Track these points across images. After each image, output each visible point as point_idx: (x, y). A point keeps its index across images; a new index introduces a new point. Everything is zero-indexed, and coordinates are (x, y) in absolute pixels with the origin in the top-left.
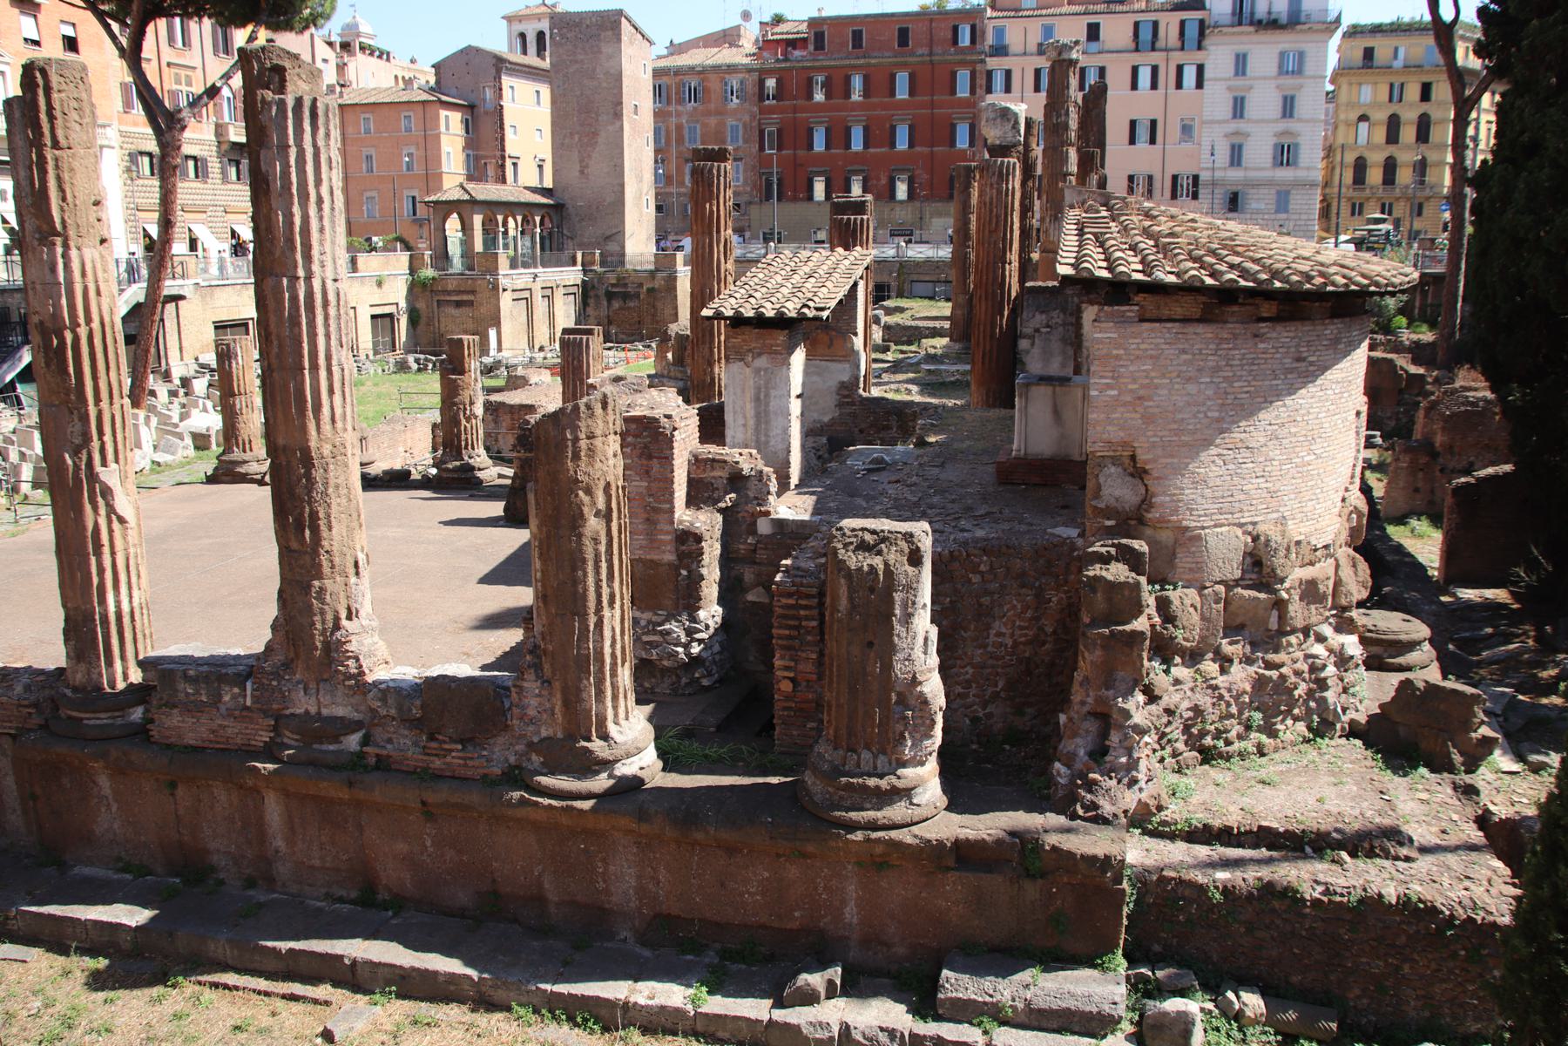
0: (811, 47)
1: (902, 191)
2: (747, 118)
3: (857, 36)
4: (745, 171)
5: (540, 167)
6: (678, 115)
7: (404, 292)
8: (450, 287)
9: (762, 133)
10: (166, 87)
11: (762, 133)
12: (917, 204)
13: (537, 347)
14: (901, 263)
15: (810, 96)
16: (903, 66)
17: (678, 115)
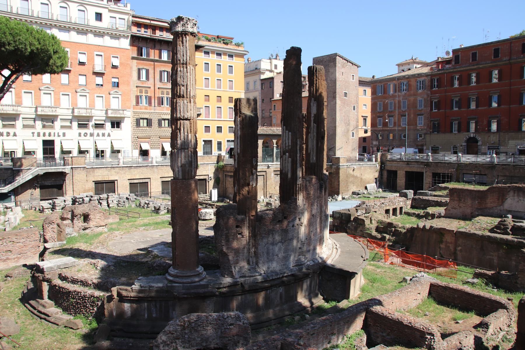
0: (453, 63)
1: (494, 127)
2: (425, 96)
3: (474, 55)
4: (424, 120)
5: (365, 119)
6: (399, 96)
7: (213, 170)
8: (228, 170)
9: (432, 102)
10: (157, 96)
11: (432, 102)
12: (502, 134)
13: (268, 196)
14: (458, 164)
15: (452, 84)
16: (495, 67)
17: (399, 96)
